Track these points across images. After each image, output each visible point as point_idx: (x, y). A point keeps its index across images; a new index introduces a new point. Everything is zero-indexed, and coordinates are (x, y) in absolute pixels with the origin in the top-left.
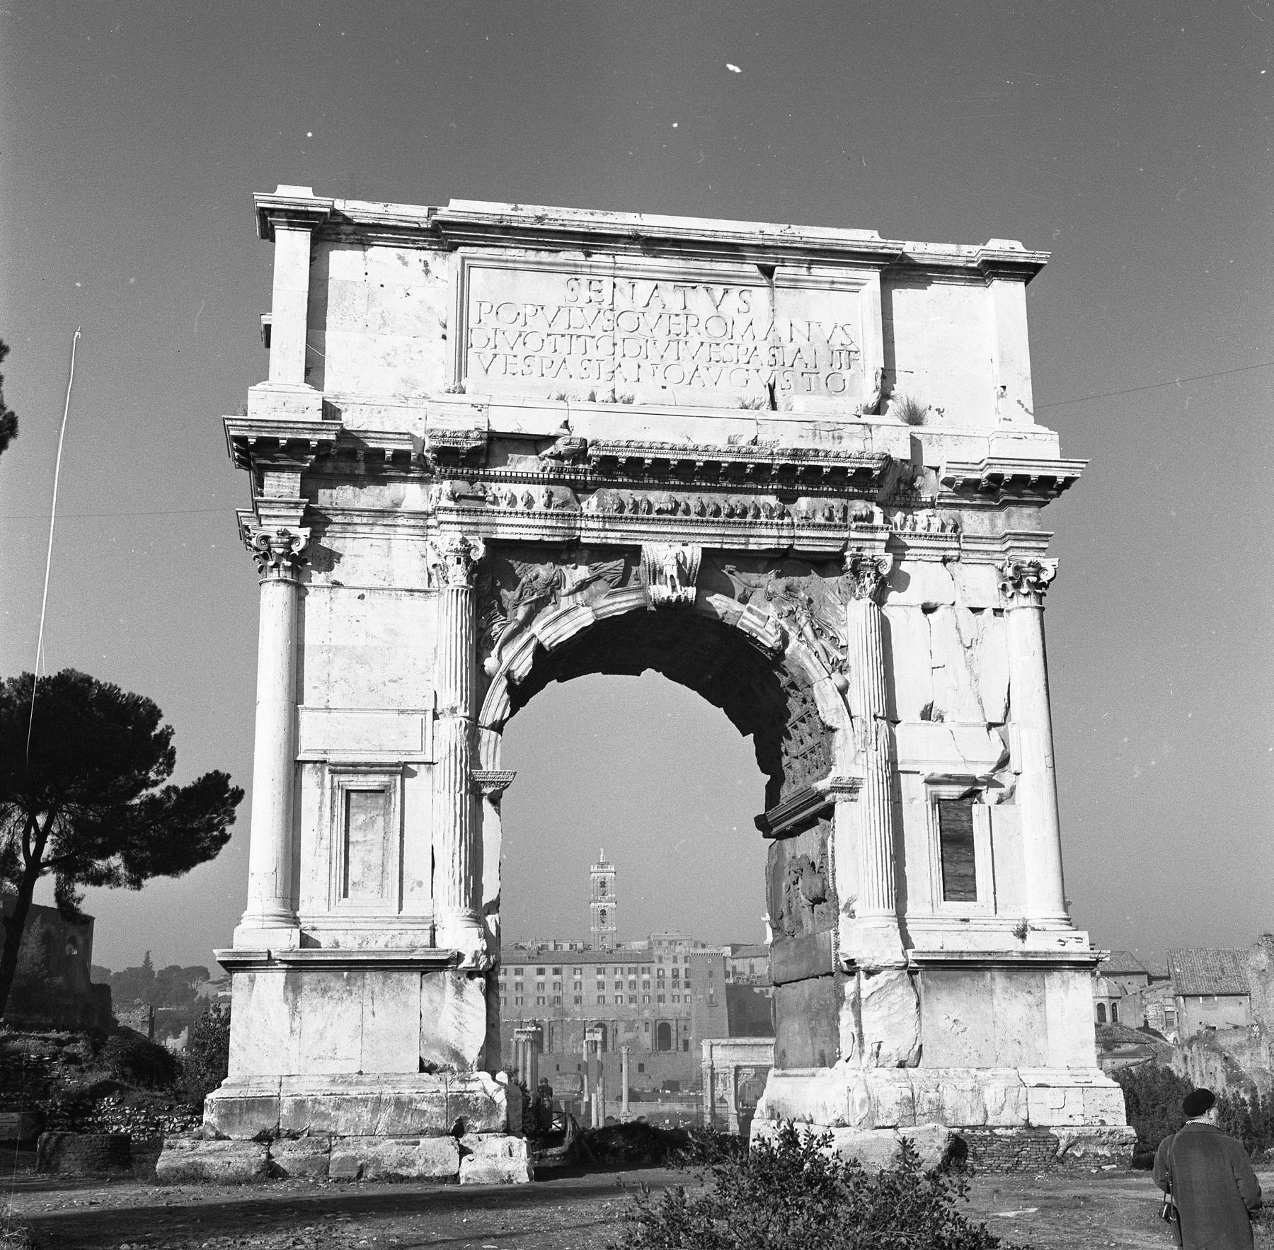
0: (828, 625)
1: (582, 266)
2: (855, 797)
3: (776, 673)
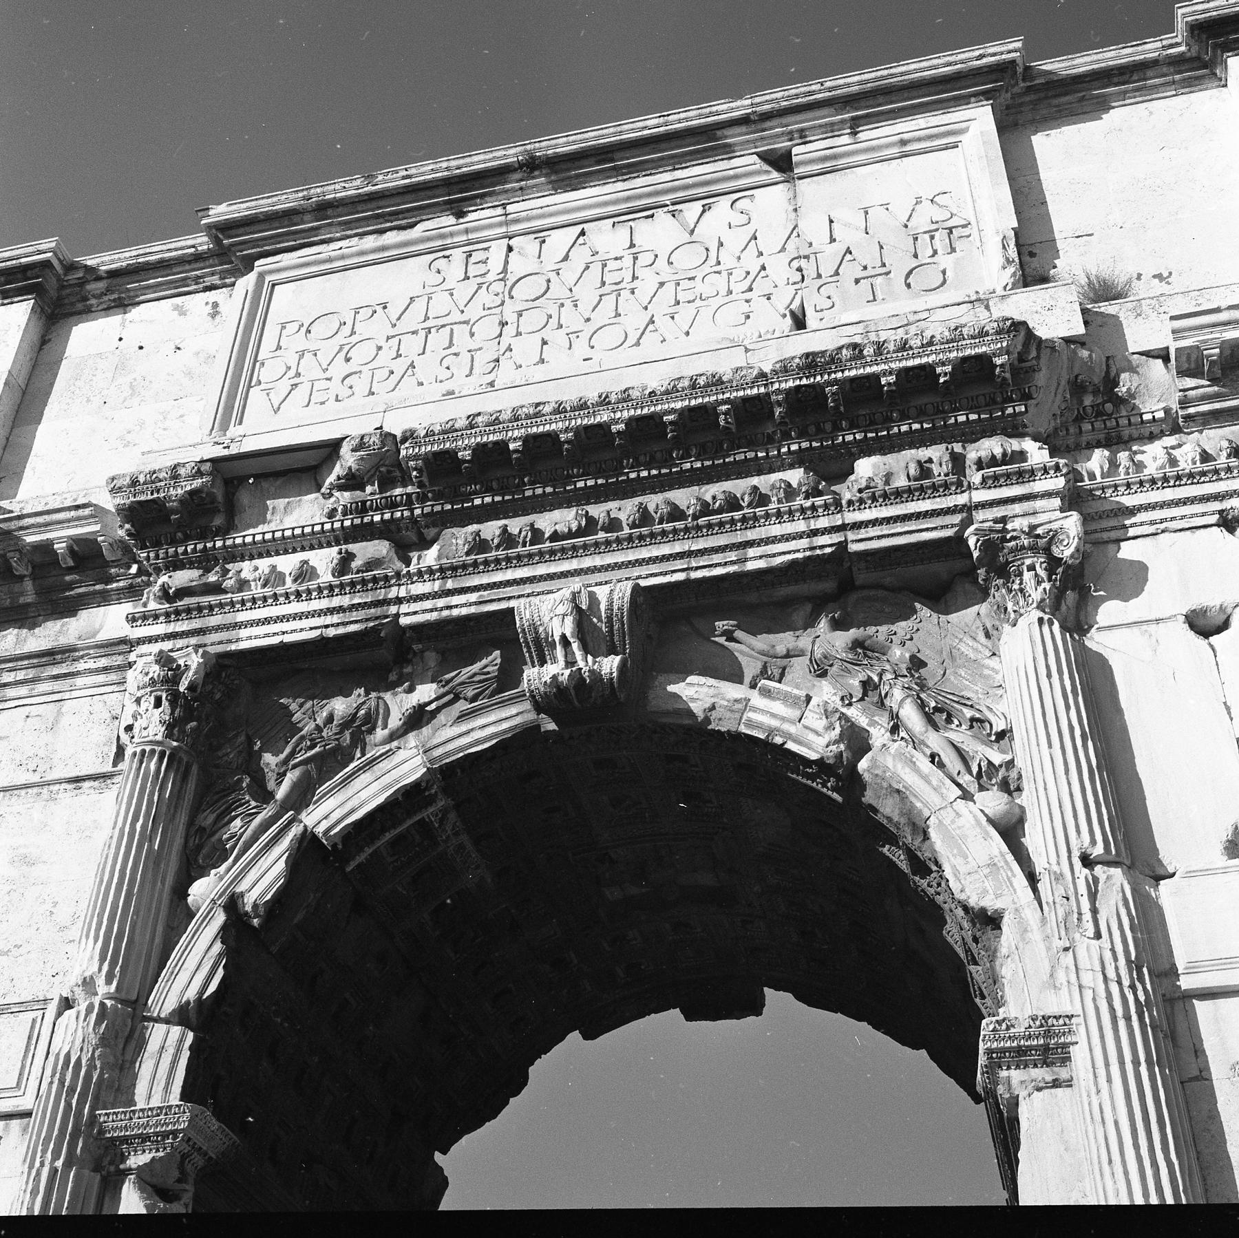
0: (965, 702)
1: (452, 235)
2: (1063, 1074)
3: (885, 850)
